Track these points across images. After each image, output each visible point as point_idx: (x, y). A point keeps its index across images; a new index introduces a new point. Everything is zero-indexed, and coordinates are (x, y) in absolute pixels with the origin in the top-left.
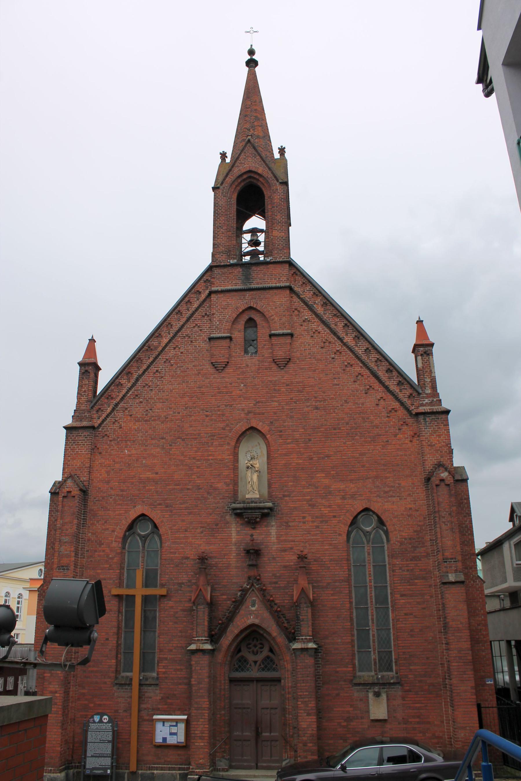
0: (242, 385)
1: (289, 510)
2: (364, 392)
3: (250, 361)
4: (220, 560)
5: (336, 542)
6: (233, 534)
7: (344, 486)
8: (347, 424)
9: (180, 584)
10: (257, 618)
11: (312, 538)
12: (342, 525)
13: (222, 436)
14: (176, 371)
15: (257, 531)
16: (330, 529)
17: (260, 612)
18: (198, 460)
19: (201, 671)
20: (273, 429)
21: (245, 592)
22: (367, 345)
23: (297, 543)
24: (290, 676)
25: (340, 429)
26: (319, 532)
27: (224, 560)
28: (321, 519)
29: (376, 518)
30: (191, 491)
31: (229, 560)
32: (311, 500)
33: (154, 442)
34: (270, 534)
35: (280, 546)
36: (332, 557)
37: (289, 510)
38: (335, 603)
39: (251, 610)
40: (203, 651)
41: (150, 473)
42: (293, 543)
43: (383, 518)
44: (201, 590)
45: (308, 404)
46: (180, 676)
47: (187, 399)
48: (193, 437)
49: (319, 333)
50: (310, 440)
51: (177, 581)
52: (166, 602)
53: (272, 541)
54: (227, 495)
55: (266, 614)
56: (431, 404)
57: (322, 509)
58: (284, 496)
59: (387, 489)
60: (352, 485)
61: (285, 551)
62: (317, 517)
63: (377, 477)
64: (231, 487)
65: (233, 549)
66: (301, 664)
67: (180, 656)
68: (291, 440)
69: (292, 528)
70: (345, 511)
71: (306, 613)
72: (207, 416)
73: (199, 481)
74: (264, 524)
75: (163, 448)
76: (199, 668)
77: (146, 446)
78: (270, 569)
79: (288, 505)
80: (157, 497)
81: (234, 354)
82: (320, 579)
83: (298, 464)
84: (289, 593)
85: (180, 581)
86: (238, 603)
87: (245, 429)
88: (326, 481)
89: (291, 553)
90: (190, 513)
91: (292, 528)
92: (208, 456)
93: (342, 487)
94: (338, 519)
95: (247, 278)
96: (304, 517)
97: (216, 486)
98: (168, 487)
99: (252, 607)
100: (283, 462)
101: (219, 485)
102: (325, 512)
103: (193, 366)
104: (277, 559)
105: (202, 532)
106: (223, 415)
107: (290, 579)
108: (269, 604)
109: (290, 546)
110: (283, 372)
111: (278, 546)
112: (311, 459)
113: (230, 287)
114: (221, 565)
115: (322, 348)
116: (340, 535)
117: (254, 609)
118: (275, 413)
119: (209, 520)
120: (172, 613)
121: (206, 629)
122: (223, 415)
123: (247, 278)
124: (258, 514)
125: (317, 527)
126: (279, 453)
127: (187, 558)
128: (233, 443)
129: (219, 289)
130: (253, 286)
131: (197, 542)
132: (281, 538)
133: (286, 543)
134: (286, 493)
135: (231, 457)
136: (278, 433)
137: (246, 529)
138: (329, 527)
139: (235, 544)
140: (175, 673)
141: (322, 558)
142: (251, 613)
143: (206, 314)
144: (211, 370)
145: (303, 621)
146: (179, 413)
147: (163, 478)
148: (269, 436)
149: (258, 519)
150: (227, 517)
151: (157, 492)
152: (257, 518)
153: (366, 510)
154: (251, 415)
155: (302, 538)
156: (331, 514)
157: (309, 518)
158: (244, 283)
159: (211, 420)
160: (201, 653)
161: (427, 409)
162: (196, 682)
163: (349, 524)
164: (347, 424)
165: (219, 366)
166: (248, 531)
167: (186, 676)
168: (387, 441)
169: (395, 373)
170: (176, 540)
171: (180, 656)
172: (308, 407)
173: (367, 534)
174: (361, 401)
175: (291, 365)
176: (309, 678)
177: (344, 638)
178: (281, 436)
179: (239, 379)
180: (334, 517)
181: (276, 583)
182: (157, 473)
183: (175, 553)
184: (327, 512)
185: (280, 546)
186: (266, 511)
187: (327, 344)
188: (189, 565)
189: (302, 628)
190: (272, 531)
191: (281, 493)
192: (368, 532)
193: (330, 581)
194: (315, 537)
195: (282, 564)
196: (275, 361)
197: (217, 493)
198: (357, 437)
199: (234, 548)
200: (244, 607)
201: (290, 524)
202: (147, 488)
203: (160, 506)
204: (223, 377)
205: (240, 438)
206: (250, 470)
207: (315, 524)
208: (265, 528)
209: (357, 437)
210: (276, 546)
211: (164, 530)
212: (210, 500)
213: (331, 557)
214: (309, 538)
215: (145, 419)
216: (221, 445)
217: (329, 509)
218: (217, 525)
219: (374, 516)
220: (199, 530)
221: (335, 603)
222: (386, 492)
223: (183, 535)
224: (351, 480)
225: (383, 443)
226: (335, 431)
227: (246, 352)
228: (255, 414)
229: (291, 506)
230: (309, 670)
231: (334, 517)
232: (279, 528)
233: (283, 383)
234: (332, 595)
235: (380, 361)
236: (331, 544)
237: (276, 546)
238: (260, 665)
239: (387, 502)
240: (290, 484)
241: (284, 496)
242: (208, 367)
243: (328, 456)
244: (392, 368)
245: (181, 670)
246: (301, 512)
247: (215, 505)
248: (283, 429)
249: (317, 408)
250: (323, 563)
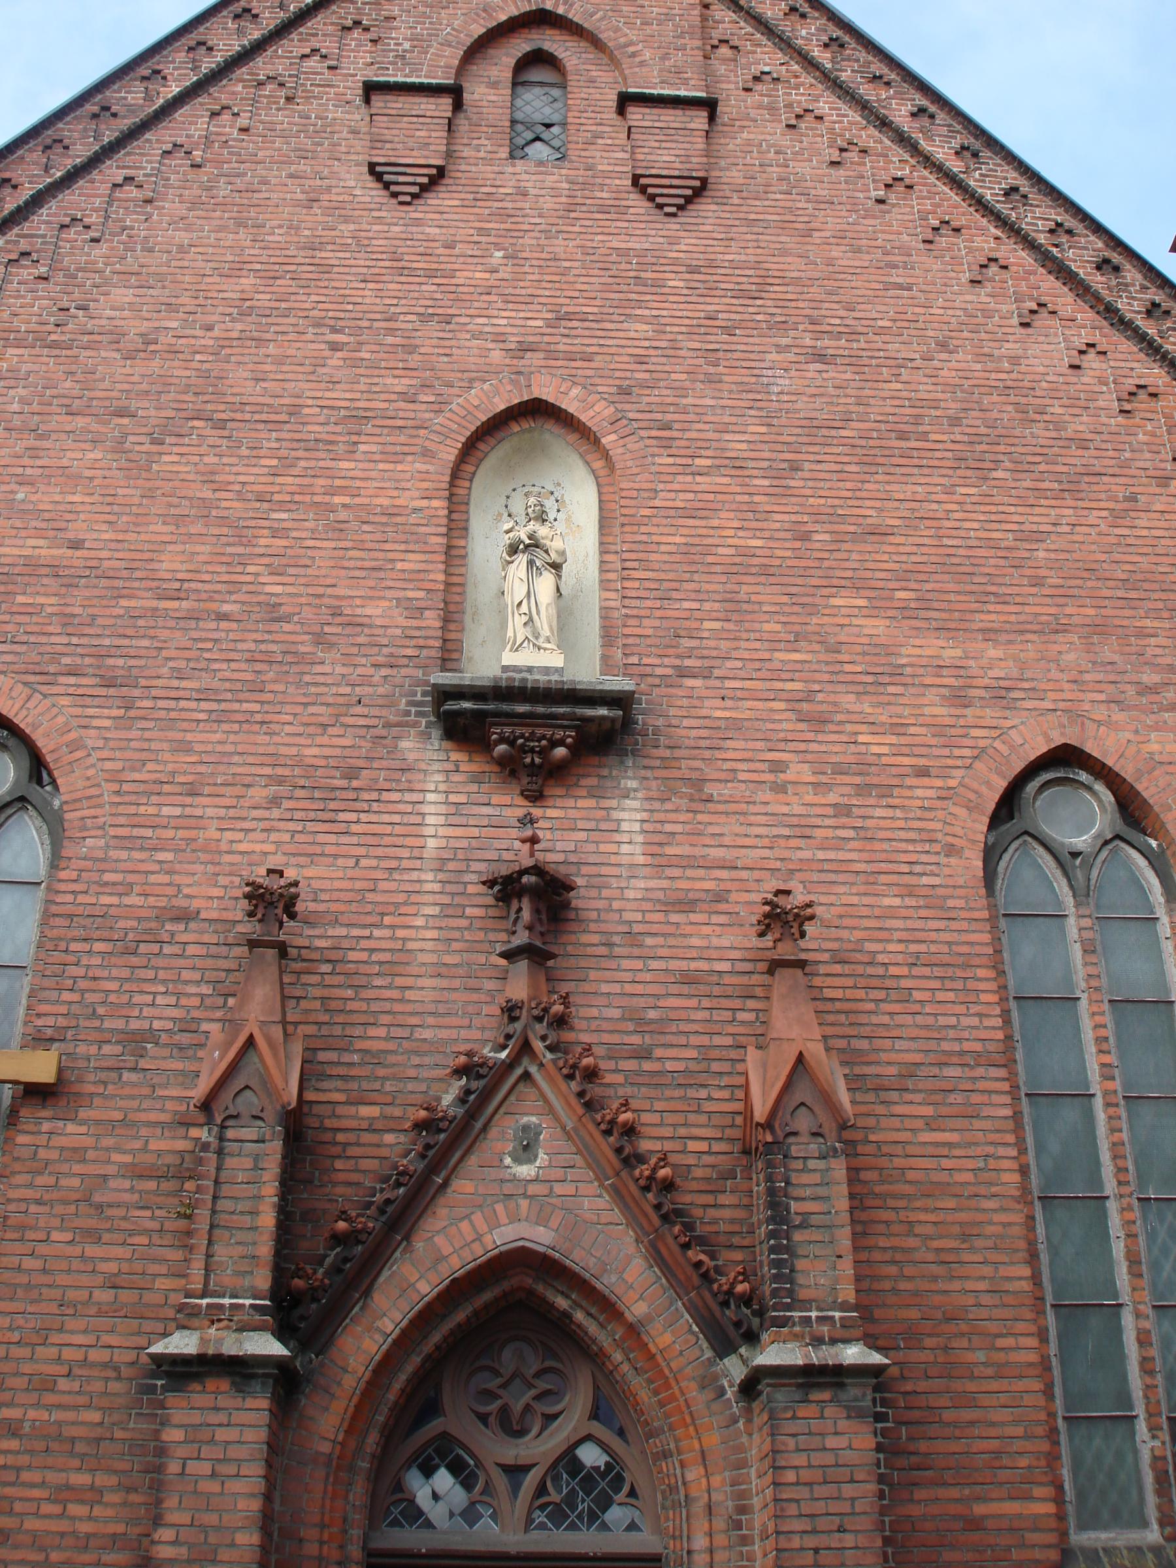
0: (500, 254)
1: (704, 733)
2: (1015, 321)
3: (538, 180)
4: (356, 932)
5: (936, 881)
6: (430, 820)
7: (958, 652)
8: (955, 421)
9: (136, 1041)
10: (543, 1220)
11: (821, 855)
12: (962, 812)
13: (400, 423)
14: (209, 189)
15: (550, 813)
16: (901, 824)
17: (558, 1189)
18: (282, 506)
19: (215, 1487)
20: (631, 415)
21: (484, 1086)
22: (1013, 177)
23: (744, 874)
24: (720, 1539)
25: (924, 436)
26: (851, 833)
27: (377, 933)
28: (858, 780)
29: (1108, 797)
30: (234, 625)
31: (400, 933)
32: (809, 697)
33: (80, 422)
34: (612, 834)
35: (665, 884)
36: (923, 948)
37: (704, 733)
38: (945, 1163)
39: (514, 1179)
40: (238, 1369)
41: (41, 542)
42: (724, 874)
43: (1147, 789)
44: (250, 1042)
45: (784, 341)
46: (85, 1528)
47: (247, 282)
48: (264, 417)
49: (819, 118)
50: (795, 467)
51: (119, 1024)
52: (46, 1126)
53: (625, 860)
54: (409, 652)
55: (595, 1203)
57: (861, 738)
58: (683, 673)
59: (1149, 678)
60: (992, 652)
61: (686, 905)
62: (839, 769)
63: (1099, 629)
64: (432, 620)
65: (429, 887)
66: (800, 1460)
67: (95, 1416)
68: (709, 462)
69: (721, 807)
70: (967, 752)
71: (820, 1185)
72: (335, 347)
73: (278, 589)
74: (585, 782)
75: (119, 447)
76: (205, 1468)
77: (41, 437)
78: (608, 999)
79: (704, 712)
80: (64, 640)
81: (467, 152)
82: (864, 1044)
83: (745, 552)
84: (709, 1106)
85: (134, 1025)
86: (446, 1141)
87: (502, 407)
88: (877, 627)
89: (715, 919)
90: (220, 718)
91: (721, 807)
92: (332, 492)
93: (951, 654)
94: (939, 783)
96: (778, 767)
97: (359, 611)
98: (124, 602)
99: (518, 1160)
100: (678, 540)
101: (374, 611)
102: (875, 749)
103: (291, 176)
104: (649, 941)
105: (275, 801)
106: (411, 349)
107: (717, 1040)
108: (619, 1144)
109: (708, 885)
110: (673, 225)
111: (652, 884)
112: (805, 537)
114: (364, 956)
115: (833, 163)
116: (951, 850)
117: (525, 1171)
118: (641, 361)
119: (314, 751)
120: (76, 1182)
121: (265, 1249)
122: (411, 349)
125: (842, 810)
126: (657, 503)
127: (185, 916)
128: (449, 454)
131: (242, 847)
132: (669, 850)
133: (689, 873)
134: (688, 662)
135: (436, 503)
136: (654, 433)
137: (495, 799)
138: (898, 813)
139: (441, 864)
140: (56, 1509)
141: (869, 946)
142: (513, 1191)
143: (357, 23)
145: (804, 1225)
146: (210, 328)
147: (106, 564)
148: (613, 437)
149: (560, 752)
150: (404, 744)
151: (67, 619)
152: (554, 744)
153: (1065, 759)
154: (534, 359)
155: (766, 853)
156: (906, 761)
157: (798, 771)
159: (355, 363)
160: (225, 1384)
162: (183, 1551)
163: (991, 806)
164: (955, 421)
165: (401, 179)
166: (507, 805)
167: (120, 1528)
168: (1133, 498)
169: (1131, 274)
170: (136, 832)
171: (95, 1416)
172: (780, 349)
173: (1067, 860)
174: (1009, 348)
175: (706, 208)
176: (849, 1540)
177: (1001, 1342)
178: (666, 444)
179: (482, 231)
180: (923, 772)
181: (643, 1054)
182: (76, 545)
183: (128, 889)
184: (885, 750)
185: (665, 884)
186: (603, 712)
187: (853, 156)
188: (191, 950)
189: (800, 1264)
190: (625, 815)
191: (666, 661)
192: (1075, 855)
193: (918, 1058)
194: (831, 855)
195: (674, 965)
196: (643, 181)
197: (361, 640)
198: (999, 474)
199: (430, 880)
200: (473, 1160)
201: (709, 789)
202: (20, 599)
203: (72, 680)
204: (418, 222)
205: (482, 446)
206: (522, 559)
207: (832, 798)
208: (592, 803)
209: (999, 474)
210: (641, 884)
211: (81, 784)
212: (327, 669)
213: (913, 948)
214: (806, 854)
215: (53, 337)
216: (396, 458)
217: (894, 739)
218: (351, 773)
219: (1099, 787)
220: (258, 794)
221: (945, 1163)
222: (1146, 690)
223: (178, 811)
224: (989, 634)
225: (1111, 505)
226: (903, 444)
228: (551, 355)
229: (719, 714)
230: (848, 1490)
231: (923, 772)
232: (657, 805)
233: (675, 262)
234: (931, 1124)
235: (1069, 232)
236: (910, 891)
237: (641, 884)
238: (541, 1490)
239: (1156, 728)
240: (707, 625)
241: (683, 673)
242: (352, 183)
243: (878, 533)
244: (1116, 258)
245: (94, 1495)
246: (760, 745)
247: (348, 690)
248: (676, 417)
250: (880, 971)
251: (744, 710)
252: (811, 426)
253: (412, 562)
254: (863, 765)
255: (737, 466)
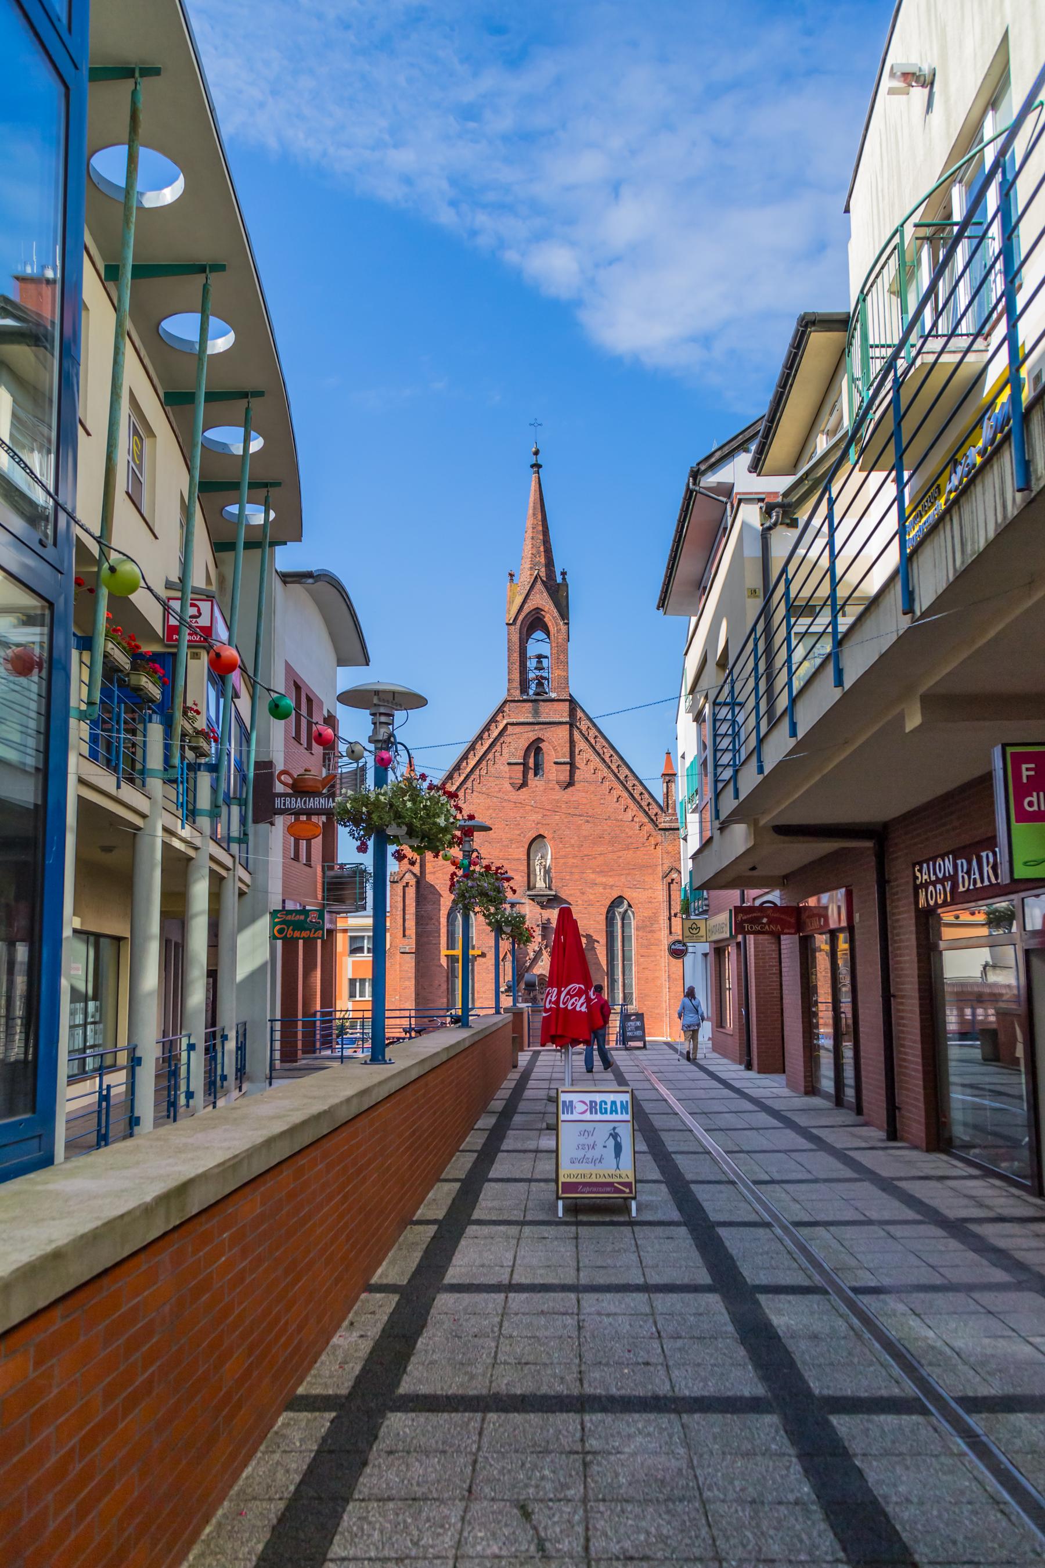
22: (627, 772)
56: (671, 821)
88: (593, 876)
95: (536, 713)
113: (522, 720)
123: (536, 713)
124: (545, 899)
129: (515, 720)
130: (541, 720)
144: (509, 788)
157: (580, 902)
158: (534, 717)
161: (667, 825)
169: (647, 796)
227: (536, 775)
249: (588, 821)
251: (572, 892)
252: (585, 837)
253: (522, 868)
254: (590, 900)
255: (573, 846)
